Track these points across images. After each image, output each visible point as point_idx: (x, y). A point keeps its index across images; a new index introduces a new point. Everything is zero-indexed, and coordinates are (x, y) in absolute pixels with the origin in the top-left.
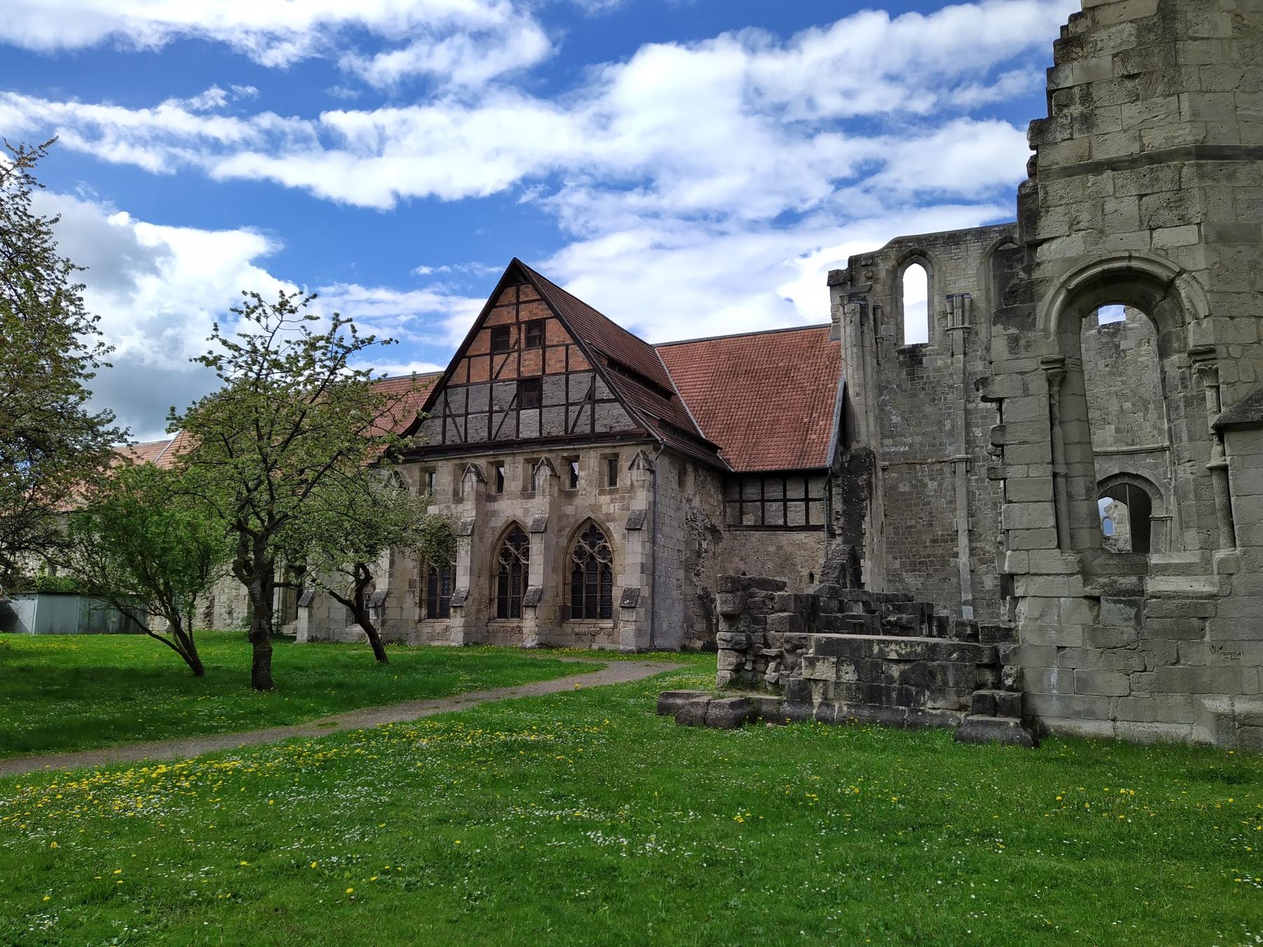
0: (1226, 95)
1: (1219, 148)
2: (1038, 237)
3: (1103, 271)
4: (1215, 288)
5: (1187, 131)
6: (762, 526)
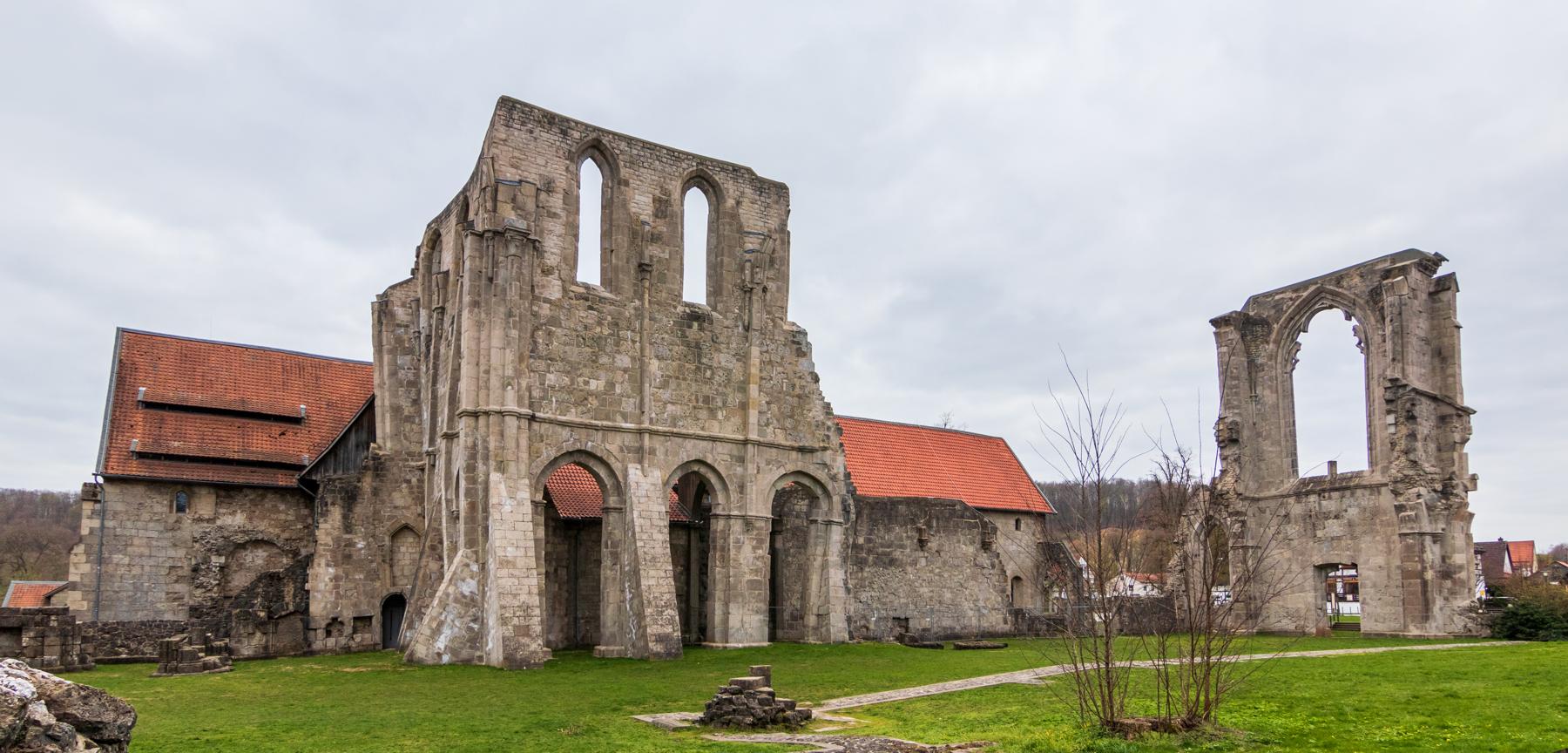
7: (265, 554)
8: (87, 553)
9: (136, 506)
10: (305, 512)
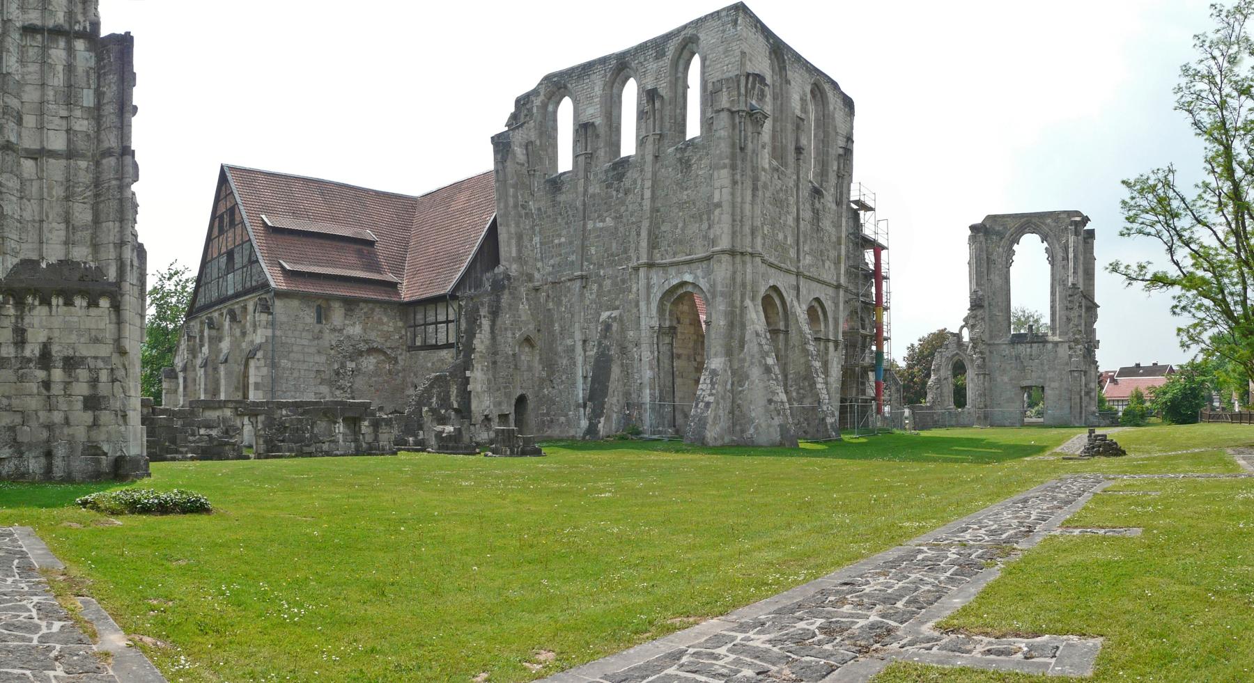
6: (427, 347)
7: (375, 361)
8: (265, 357)
9: (293, 318)
10: (400, 324)
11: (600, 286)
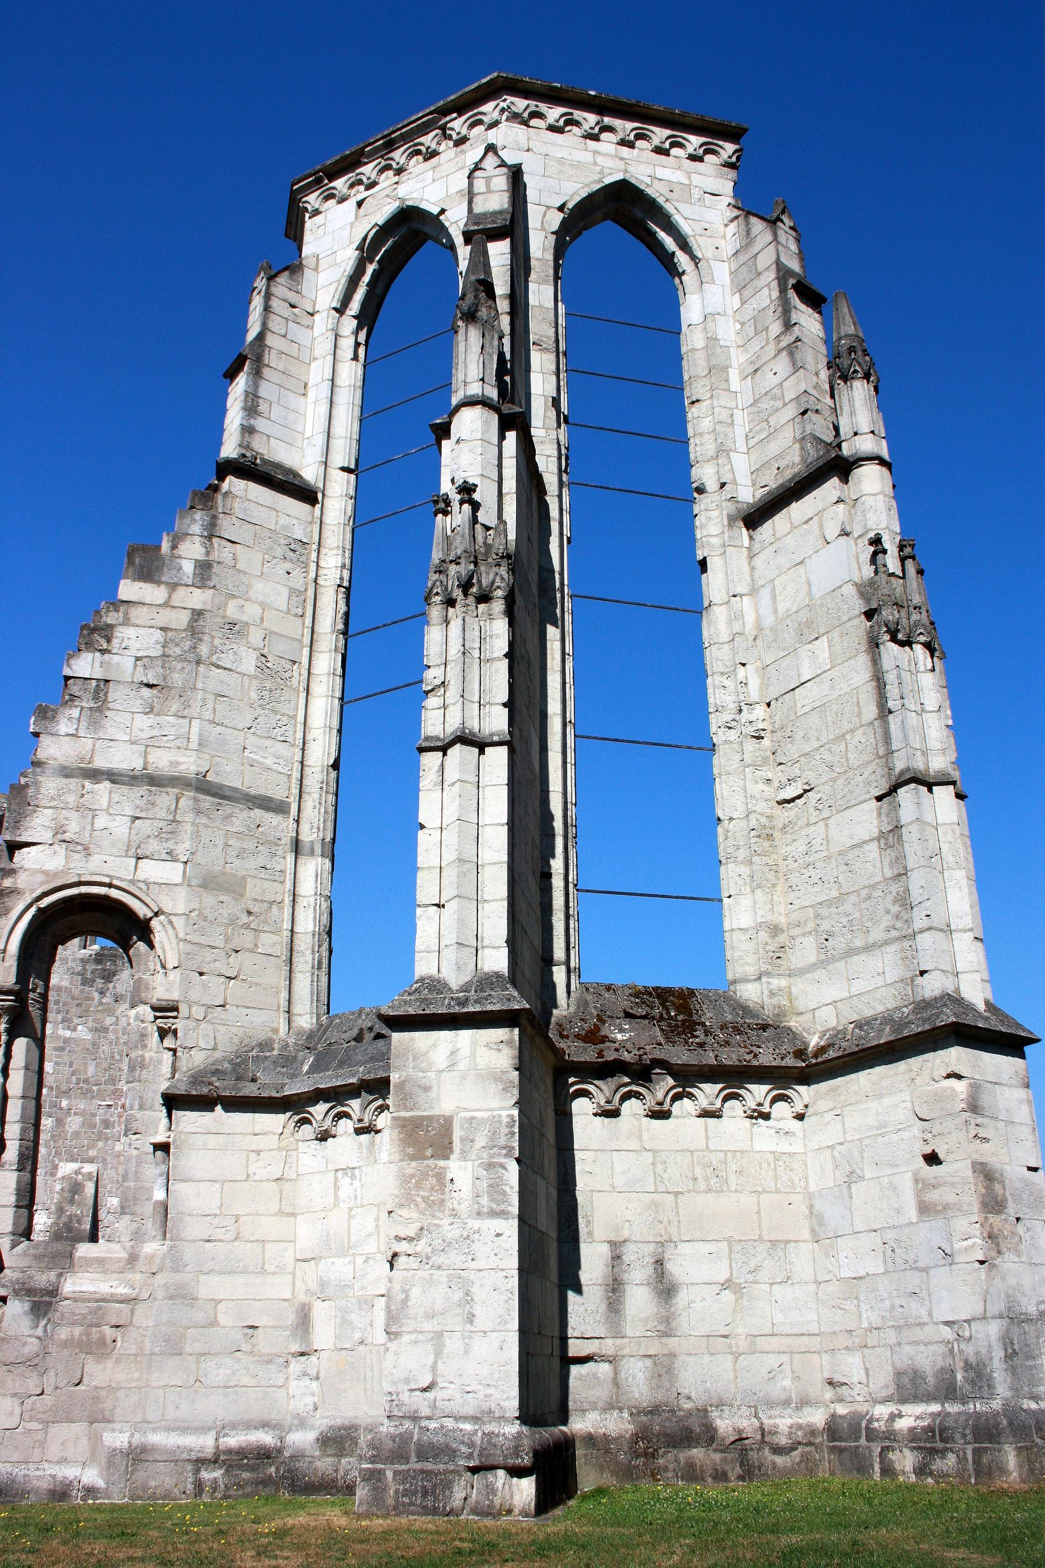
0: (237, 733)
1: (221, 787)
2: (18, 839)
3: (80, 895)
4: (188, 937)
5: (193, 759)
11: (60, 1122)
